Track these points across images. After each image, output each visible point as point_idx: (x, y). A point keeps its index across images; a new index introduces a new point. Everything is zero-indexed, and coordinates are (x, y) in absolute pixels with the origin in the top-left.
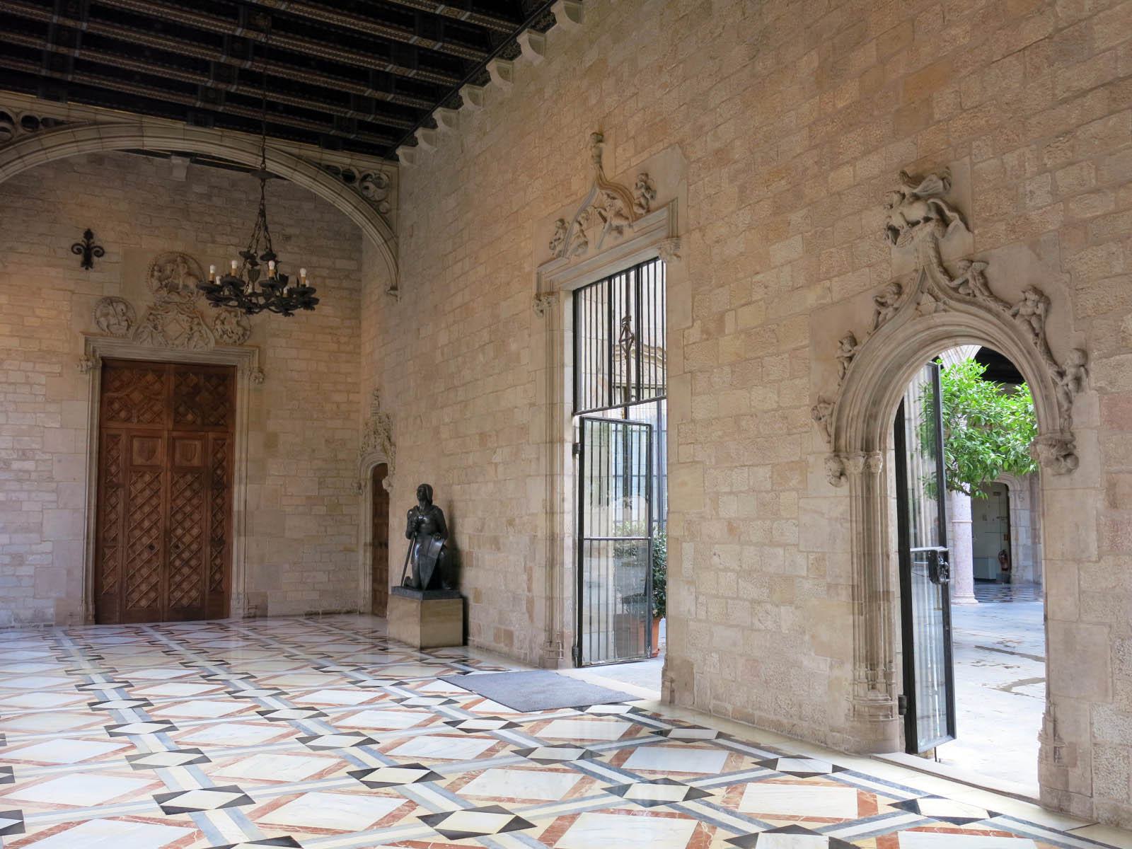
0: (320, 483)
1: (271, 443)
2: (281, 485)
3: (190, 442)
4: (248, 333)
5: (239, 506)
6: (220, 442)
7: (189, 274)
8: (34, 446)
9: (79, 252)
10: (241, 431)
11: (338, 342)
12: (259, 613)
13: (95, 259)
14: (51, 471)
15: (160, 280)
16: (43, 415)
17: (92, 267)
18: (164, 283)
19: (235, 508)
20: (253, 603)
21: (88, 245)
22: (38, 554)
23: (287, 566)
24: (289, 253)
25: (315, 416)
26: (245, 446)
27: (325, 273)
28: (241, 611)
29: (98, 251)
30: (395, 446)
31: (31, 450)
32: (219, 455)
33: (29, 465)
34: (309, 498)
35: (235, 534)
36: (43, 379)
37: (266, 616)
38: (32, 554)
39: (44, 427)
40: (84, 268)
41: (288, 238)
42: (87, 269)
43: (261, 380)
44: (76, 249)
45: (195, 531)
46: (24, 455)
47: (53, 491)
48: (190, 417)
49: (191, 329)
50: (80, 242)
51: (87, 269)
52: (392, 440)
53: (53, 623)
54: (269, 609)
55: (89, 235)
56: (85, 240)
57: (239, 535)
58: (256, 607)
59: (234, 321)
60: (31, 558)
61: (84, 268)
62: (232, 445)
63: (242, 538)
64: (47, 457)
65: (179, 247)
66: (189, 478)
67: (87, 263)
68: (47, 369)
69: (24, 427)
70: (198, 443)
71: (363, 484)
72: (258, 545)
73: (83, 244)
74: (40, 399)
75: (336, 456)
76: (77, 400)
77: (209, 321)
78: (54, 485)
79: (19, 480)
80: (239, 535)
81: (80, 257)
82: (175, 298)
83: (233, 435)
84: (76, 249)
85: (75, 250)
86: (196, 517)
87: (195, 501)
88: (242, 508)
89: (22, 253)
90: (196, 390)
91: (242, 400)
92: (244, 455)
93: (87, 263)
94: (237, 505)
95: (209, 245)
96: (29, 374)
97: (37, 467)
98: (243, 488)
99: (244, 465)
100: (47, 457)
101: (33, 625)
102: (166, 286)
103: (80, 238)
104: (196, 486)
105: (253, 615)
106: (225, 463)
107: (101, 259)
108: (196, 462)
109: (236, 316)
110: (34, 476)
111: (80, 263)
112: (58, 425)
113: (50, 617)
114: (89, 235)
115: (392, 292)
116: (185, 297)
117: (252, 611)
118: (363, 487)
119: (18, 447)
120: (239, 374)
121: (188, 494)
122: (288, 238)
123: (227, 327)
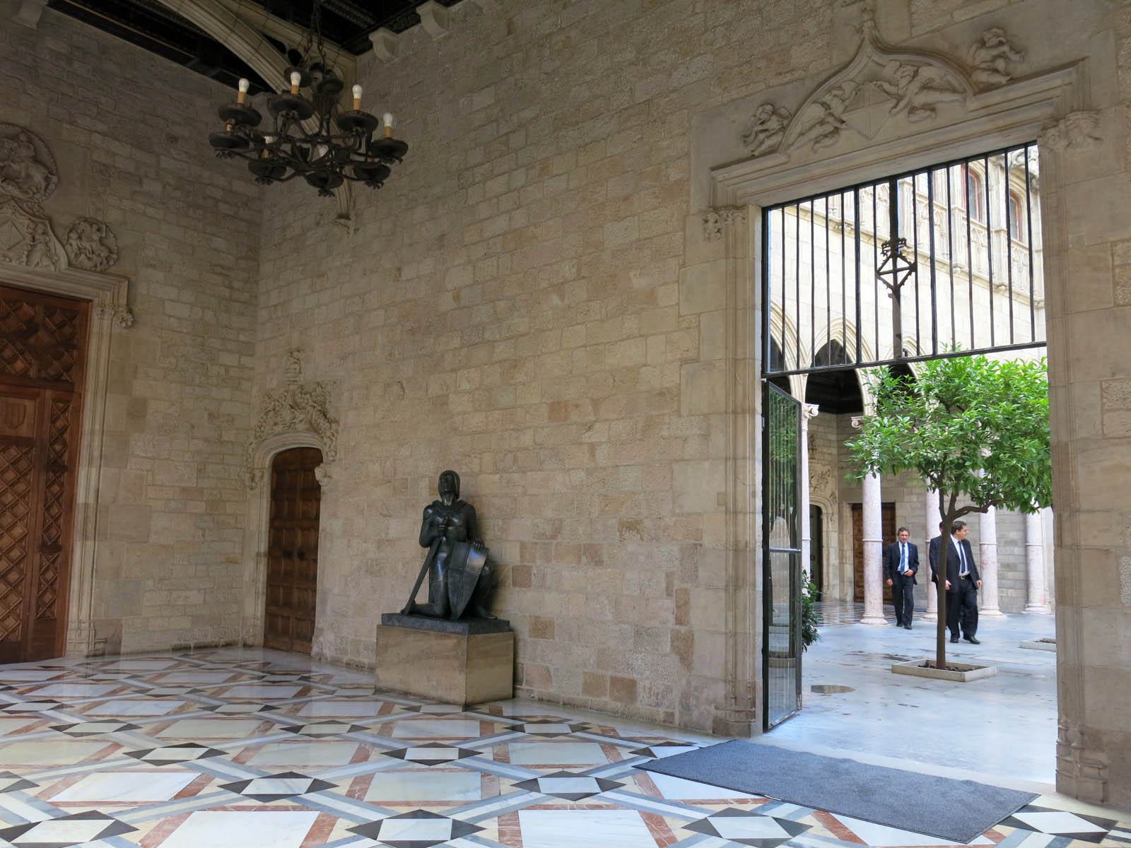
0: (199, 471)
1: (137, 412)
2: (148, 471)
3: (17, 401)
4: (115, 256)
5: (87, 496)
6: (61, 405)
7: (36, 160)
10: (95, 394)
11: (231, 288)
12: (109, 648)
19: (81, 497)
20: (101, 636)
23: (150, 583)
24: (173, 158)
26: (97, 415)
27: (219, 194)
28: (84, 647)
30: (337, 422)
32: (60, 424)
34: (184, 490)
37: (118, 654)
41: (173, 139)
43: (129, 323)
45: (18, 531)
48: (19, 365)
49: (34, 239)
52: (331, 415)
54: (123, 644)
57: (85, 537)
58: (106, 641)
59: (95, 237)
62: (78, 411)
63: (90, 543)
65: (23, 119)
66: (13, 452)
70: (29, 405)
71: (258, 474)
72: (112, 554)
75: (221, 436)
77: (60, 231)
80: (85, 537)
83: (81, 396)
86: (21, 509)
87: (21, 487)
88: (91, 501)
90: (31, 328)
91: (99, 350)
92: (97, 427)
94: (83, 495)
95: (65, 125)
98: (94, 471)
99: (97, 439)
104: (23, 464)
105: (100, 652)
106: (66, 436)
108: (24, 431)
115: (342, 221)
116: (26, 192)
117: (100, 646)
118: (257, 479)
120: (95, 316)
121: (10, 475)
122: (173, 139)
123: (86, 244)
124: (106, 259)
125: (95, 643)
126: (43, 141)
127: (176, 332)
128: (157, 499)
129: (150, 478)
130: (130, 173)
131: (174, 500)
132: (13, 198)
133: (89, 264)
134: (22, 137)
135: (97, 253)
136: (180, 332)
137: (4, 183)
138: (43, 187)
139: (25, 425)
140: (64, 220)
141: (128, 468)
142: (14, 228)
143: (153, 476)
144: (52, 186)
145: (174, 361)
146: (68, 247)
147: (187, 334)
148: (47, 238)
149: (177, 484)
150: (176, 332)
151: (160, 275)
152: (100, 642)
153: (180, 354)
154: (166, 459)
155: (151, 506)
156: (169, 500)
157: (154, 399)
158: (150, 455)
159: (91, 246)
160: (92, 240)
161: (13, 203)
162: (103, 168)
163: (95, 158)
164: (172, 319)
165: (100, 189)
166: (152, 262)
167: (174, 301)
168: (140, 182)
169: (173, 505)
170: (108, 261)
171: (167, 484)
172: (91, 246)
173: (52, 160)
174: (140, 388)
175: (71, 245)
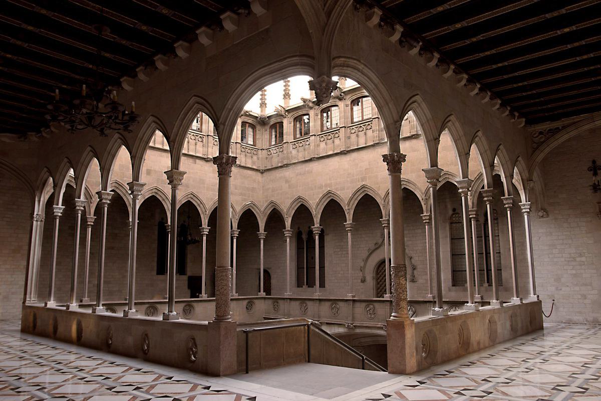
8: (584, 251)
9: (591, 170)
14: (592, 261)
16: (586, 238)
31: (584, 253)
33: (583, 259)
44: (590, 169)
46: (581, 255)
55: (594, 162)
64: (590, 255)
79: (581, 265)
81: (592, 172)
84: (590, 169)
103: (590, 164)
114: (594, 162)
119: (578, 252)
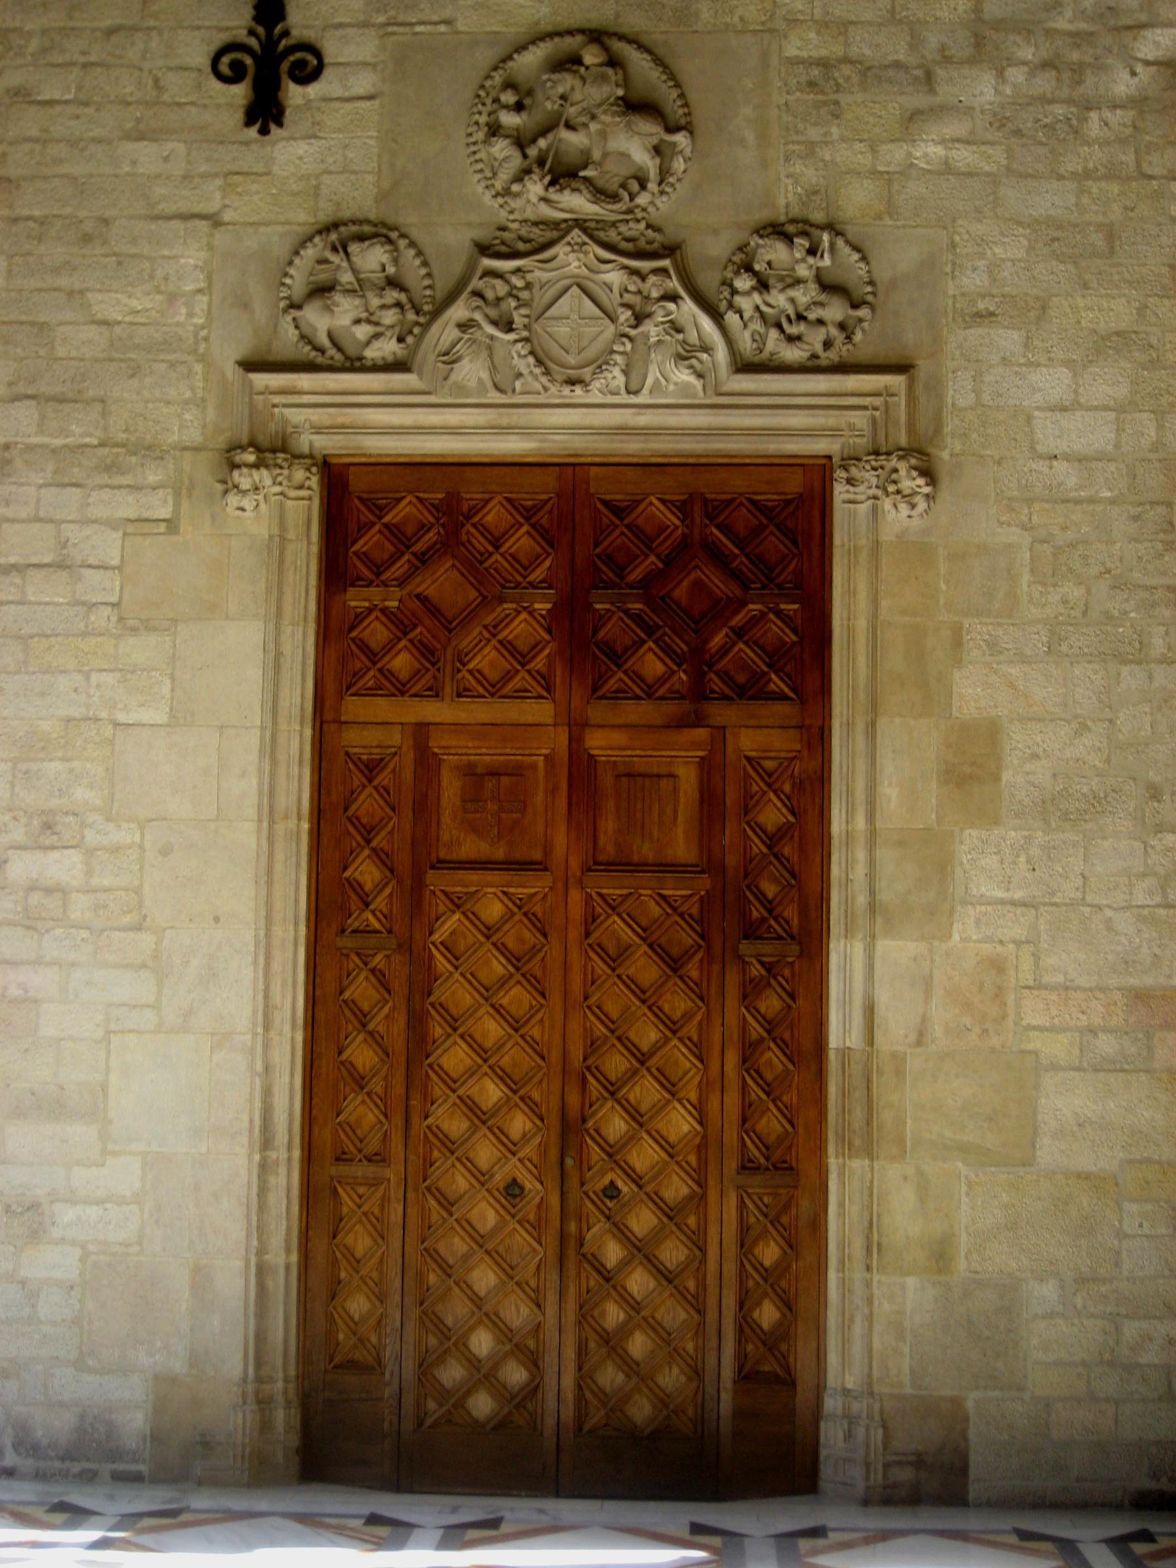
1: (971, 768)
2: (1018, 943)
9: (236, 75)
13: (294, 94)
14: (138, 891)
15: (521, 142)
16: (109, 678)
17: (280, 124)
18: (533, 152)
19: (834, 1039)
21: (269, 44)
22: (88, 1201)
25: (1158, 645)
26: (880, 781)
29: (302, 64)
33: (62, 867)
35: (831, 1149)
36: (109, 546)
38: (72, 1200)
39: (116, 724)
40: (253, 132)
42: (264, 131)
44: (227, 64)
47: (144, 966)
50: (242, 35)
51: (264, 131)
53: (143, 1468)
54: (973, 1472)
56: (261, 30)
60: (67, 1214)
61: (253, 132)
64: (125, 835)
67: (265, 112)
68: (128, 506)
69: (45, 726)
73: (253, 42)
74: (102, 617)
76: (227, 618)
77: (709, 280)
78: (146, 940)
81: (240, 92)
82: (577, 202)
84: (227, 64)
85: (224, 68)
89: (51, 103)
93: (265, 112)
94: (842, 1030)
96: (69, 531)
97: (89, 873)
99: (861, 855)
100: (125, 835)
101: (76, 1468)
102: (541, 162)
107: (313, 90)
109: (812, 251)
110: (80, 905)
111: (240, 115)
112: (161, 717)
113: (131, 1443)
117: (905, 1475)
120: (840, 491)
124: (842, 326)
125: (887, 1466)
126: (649, 51)
127: (1077, 502)
128: (1052, 1029)
129: (1027, 964)
130: (897, 65)
131: (1105, 1030)
132: (579, 223)
133: (793, 354)
134: (592, 56)
135: (812, 316)
136: (1091, 501)
137: (551, 189)
138: (653, 174)
139: (680, 831)
140: (712, 248)
141: (956, 937)
142: (587, 302)
143: (1036, 957)
144: (679, 165)
145: (1076, 593)
146: (732, 318)
147: (1112, 502)
148: (671, 306)
149: (1113, 981)
150: (1077, 502)
151: (1008, 339)
152: (900, 1463)
153: (1094, 571)
154: (1073, 904)
155: (1036, 1053)
156: (1093, 1031)
157: (1022, 719)
158: (1018, 895)
159: (792, 300)
160: (798, 282)
161: (576, 235)
162: (815, 72)
163: (791, 51)
164: (1060, 466)
165: (814, 134)
166: (981, 306)
167: (1064, 409)
168: (929, 76)
169: (1106, 1045)
170: (857, 325)
171: (1083, 982)
172: (792, 300)
173: (674, 93)
174: (972, 692)
175: (740, 312)
